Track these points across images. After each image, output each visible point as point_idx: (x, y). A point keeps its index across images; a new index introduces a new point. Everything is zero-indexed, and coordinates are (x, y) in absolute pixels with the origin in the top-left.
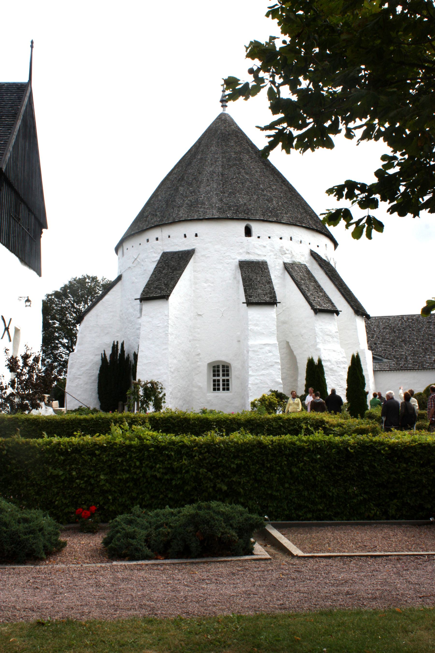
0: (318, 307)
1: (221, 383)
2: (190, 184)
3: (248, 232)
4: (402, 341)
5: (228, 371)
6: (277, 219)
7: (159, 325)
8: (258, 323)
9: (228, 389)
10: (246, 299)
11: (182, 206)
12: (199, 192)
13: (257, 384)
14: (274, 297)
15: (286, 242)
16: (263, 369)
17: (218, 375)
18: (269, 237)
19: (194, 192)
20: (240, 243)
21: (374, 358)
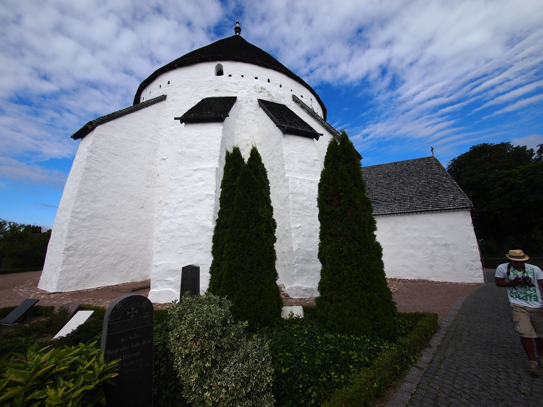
3: (220, 72)
4: (401, 184)
8: (194, 143)
16: (185, 207)
18: (242, 76)
20: (209, 82)
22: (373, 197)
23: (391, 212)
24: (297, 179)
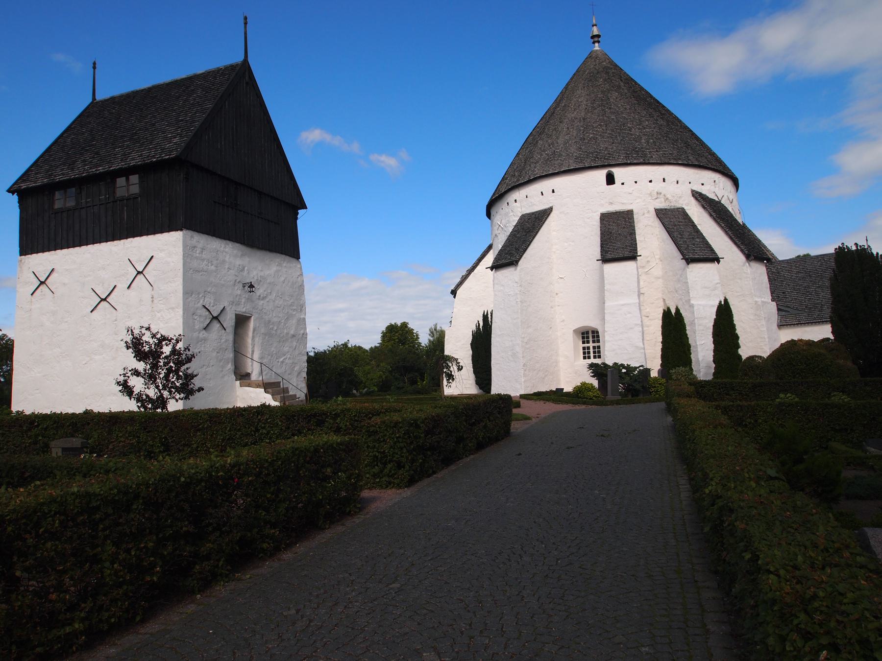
0: (691, 256)
1: (591, 350)
2: (550, 136)
3: (610, 180)
4: (819, 287)
5: (598, 336)
6: (644, 160)
7: (510, 293)
10: (601, 255)
11: (537, 162)
12: (557, 143)
13: (614, 350)
14: (635, 249)
15: (658, 186)
16: (621, 333)
17: (588, 342)
18: (636, 182)
19: (553, 144)
21: (779, 310)
22: (786, 304)
23: (798, 322)
24: (700, 305)
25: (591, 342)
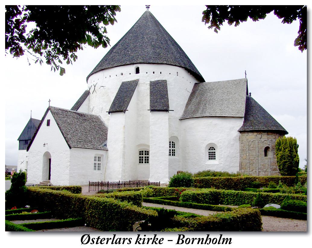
1: (144, 159)
9: (148, 162)
17: (143, 154)
25: (144, 154)
